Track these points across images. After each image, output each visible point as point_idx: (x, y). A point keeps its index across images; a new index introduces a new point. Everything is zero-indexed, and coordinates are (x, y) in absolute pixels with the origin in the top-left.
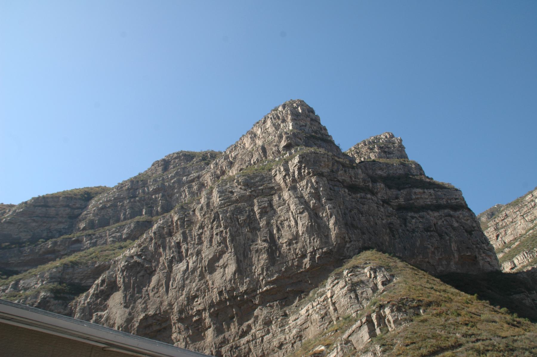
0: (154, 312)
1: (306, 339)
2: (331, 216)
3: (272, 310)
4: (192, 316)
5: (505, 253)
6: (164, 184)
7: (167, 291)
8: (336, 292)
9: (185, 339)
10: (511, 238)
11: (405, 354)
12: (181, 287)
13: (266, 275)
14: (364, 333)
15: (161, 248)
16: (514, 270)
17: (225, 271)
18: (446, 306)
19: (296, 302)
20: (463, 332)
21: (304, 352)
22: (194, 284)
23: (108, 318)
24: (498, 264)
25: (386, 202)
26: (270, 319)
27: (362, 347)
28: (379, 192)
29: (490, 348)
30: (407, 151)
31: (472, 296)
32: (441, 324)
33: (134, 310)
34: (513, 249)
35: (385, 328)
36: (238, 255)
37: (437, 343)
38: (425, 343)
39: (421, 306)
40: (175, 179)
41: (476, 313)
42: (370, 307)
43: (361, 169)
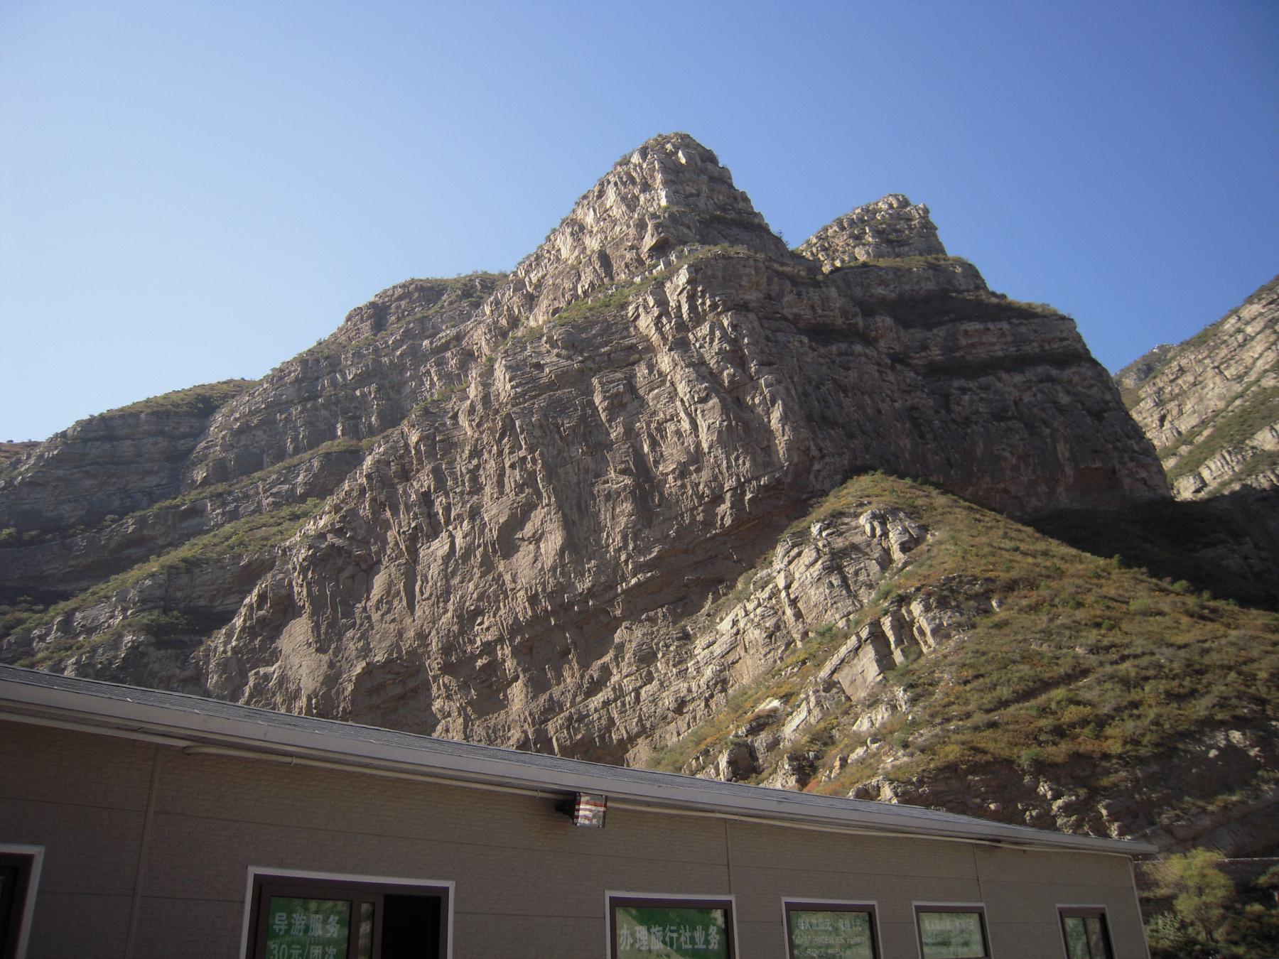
1: (737, 686)
2: (773, 403)
3: (655, 629)
4: (474, 657)
5: (1181, 456)
7: (411, 607)
8: (797, 575)
9: (462, 710)
10: (1194, 421)
11: (961, 701)
12: (441, 594)
14: (868, 664)
15: (387, 509)
16: (1202, 495)
17: (538, 548)
18: (1049, 587)
19: (708, 605)
20: (1089, 642)
21: (733, 716)
22: (471, 586)
23: (283, 680)
24: (1165, 482)
25: (899, 359)
26: (652, 648)
27: (863, 694)
28: (882, 336)
29: (1151, 672)
30: (942, 235)
31: (1108, 561)
32: (1039, 628)
34: (1199, 447)
35: (914, 648)
36: (567, 511)
37: (1032, 673)
38: (1006, 673)
39: (992, 591)
41: (1119, 599)
42: (875, 603)
43: (838, 287)
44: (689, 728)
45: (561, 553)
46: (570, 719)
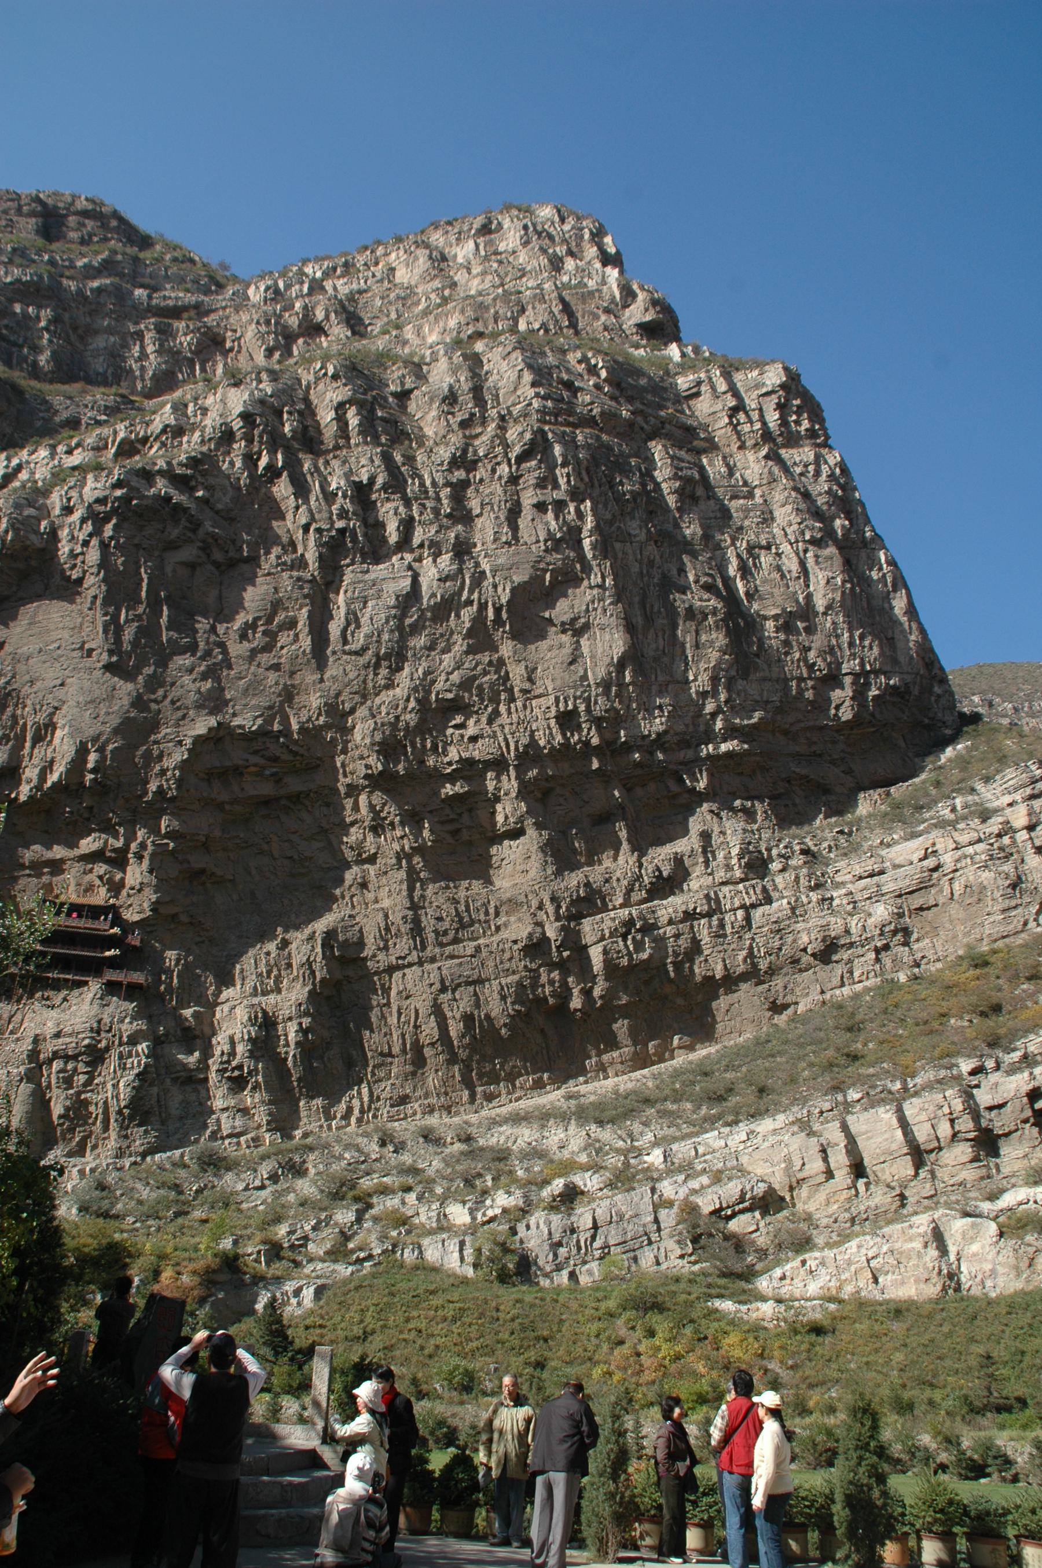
0: (259, 721)
6: (60, 283)
12: (388, 656)
13: (726, 702)
33: (161, 692)
40: (108, 282)
44: (843, 985)
45: (621, 666)
46: (629, 923)
